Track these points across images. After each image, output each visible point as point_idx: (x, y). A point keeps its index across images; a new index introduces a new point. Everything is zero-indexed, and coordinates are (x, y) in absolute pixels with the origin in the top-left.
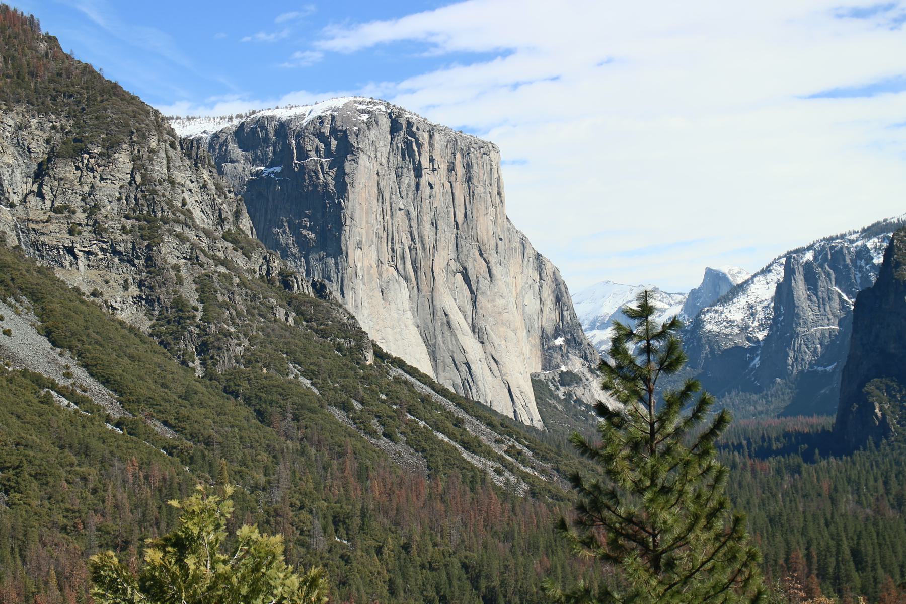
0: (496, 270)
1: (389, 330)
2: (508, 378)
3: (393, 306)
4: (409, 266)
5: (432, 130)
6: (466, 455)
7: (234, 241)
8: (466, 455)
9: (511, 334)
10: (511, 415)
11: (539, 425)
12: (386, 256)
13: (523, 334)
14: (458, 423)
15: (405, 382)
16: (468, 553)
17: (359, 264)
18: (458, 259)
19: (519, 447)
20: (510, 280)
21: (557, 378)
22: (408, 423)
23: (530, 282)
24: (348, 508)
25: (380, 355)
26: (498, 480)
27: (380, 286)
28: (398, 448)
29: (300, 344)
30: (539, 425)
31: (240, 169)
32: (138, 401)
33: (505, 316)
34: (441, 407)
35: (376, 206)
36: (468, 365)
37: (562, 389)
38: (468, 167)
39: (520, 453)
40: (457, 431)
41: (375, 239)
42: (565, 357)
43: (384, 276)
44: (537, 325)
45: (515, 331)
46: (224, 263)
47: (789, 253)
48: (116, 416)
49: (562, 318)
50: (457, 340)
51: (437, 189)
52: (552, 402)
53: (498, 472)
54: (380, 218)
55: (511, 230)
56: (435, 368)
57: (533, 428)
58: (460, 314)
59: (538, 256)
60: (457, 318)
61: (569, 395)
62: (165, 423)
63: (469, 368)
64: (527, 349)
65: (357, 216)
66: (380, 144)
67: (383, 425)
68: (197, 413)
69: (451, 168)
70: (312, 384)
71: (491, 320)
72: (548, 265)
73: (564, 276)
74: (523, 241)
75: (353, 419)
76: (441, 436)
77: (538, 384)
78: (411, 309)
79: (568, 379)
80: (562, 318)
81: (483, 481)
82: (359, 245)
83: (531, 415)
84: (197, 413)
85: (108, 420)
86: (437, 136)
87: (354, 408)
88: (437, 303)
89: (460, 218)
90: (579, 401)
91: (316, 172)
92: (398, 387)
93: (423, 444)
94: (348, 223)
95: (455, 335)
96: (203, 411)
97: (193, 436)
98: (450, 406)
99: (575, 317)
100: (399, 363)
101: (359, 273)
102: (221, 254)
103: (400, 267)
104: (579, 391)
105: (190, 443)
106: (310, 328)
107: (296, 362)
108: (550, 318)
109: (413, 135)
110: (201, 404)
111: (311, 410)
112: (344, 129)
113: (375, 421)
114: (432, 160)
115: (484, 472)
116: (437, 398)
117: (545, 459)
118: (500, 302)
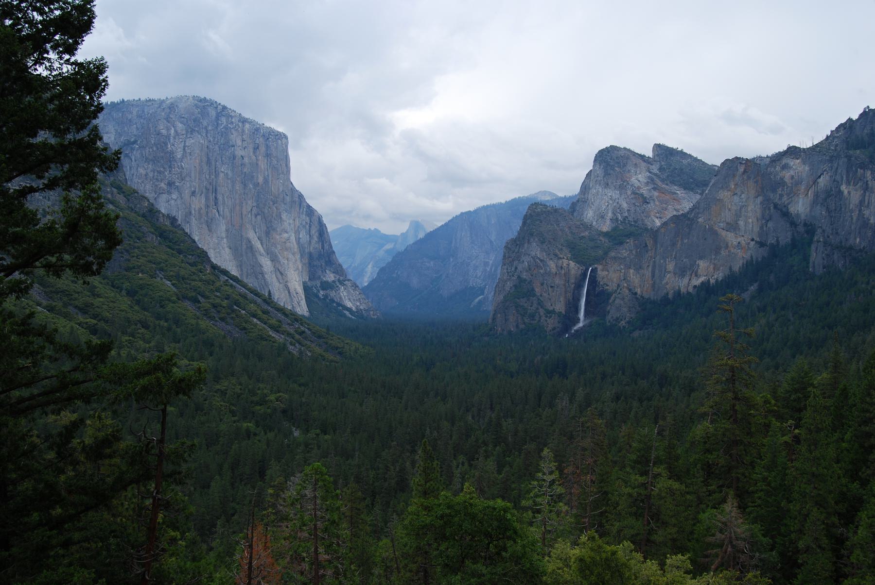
0: (284, 216)
1: (212, 251)
2: (289, 284)
3: (215, 235)
4: (226, 210)
5: (244, 121)
6: (271, 333)
7: (120, 189)
8: (271, 333)
9: (291, 256)
10: (289, 308)
11: (306, 314)
12: (212, 203)
13: (298, 257)
14: (265, 312)
15: (231, 286)
16: (281, 394)
17: (193, 206)
18: (258, 207)
19: (303, 328)
20: (291, 221)
21: (319, 285)
22: (233, 311)
23: (304, 223)
24: (203, 366)
25: (214, 267)
26: (294, 350)
27: (207, 221)
28: (229, 328)
29: (163, 257)
30: (306, 314)
31: (113, 139)
32: (57, 293)
33: (288, 244)
34: (255, 303)
35: (205, 168)
36: (262, 274)
37: (322, 292)
38: (267, 147)
39: (303, 332)
40: (265, 317)
41: (204, 190)
42: (324, 271)
43: (210, 214)
44: (306, 251)
45: (294, 254)
46: (112, 203)
47: (462, 214)
48: (45, 303)
49: (323, 248)
50: (256, 259)
51: (246, 160)
52: (316, 300)
53: (291, 344)
54: (208, 177)
55: (293, 190)
56: (241, 275)
57: (304, 316)
58: (259, 242)
59: (309, 207)
60: (258, 245)
61: (326, 296)
62: (76, 307)
63: (263, 276)
64: (300, 267)
65: (193, 175)
66: (210, 128)
67: (219, 312)
68: (97, 301)
69: (256, 148)
70: (173, 284)
71: (279, 247)
72: (316, 214)
73: (325, 220)
74: (301, 196)
75: (199, 308)
76: (255, 320)
77: (306, 289)
78: (227, 237)
79: (326, 286)
80: (323, 248)
81: (284, 347)
82: (193, 193)
83: (302, 309)
84: (97, 301)
85: (39, 305)
86: (247, 126)
87: (199, 302)
88: (244, 234)
89: (261, 180)
90: (332, 301)
91: (166, 144)
92: (227, 288)
93: (244, 324)
94: (188, 179)
95: (254, 255)
96: (101, 300)
97: (95, 317)
98: (259, 300)
99: (331, 247)
100: (225, 272)
101: (193, 212)
102: (109, 196)
103: (221, 209)
104: (332, 294)
105: (95, 322)
106: (170, 247)
107: (161, 270)
108: (315, 245)
109: (232, 123)
110: (99, 296)
111: (169, 300)
112: (186, 116)
113: (213, 310)
114: (243, 140)
115: (285, 345)
116: (251, 296)
117: (320, 337)
118: (286, 235)
